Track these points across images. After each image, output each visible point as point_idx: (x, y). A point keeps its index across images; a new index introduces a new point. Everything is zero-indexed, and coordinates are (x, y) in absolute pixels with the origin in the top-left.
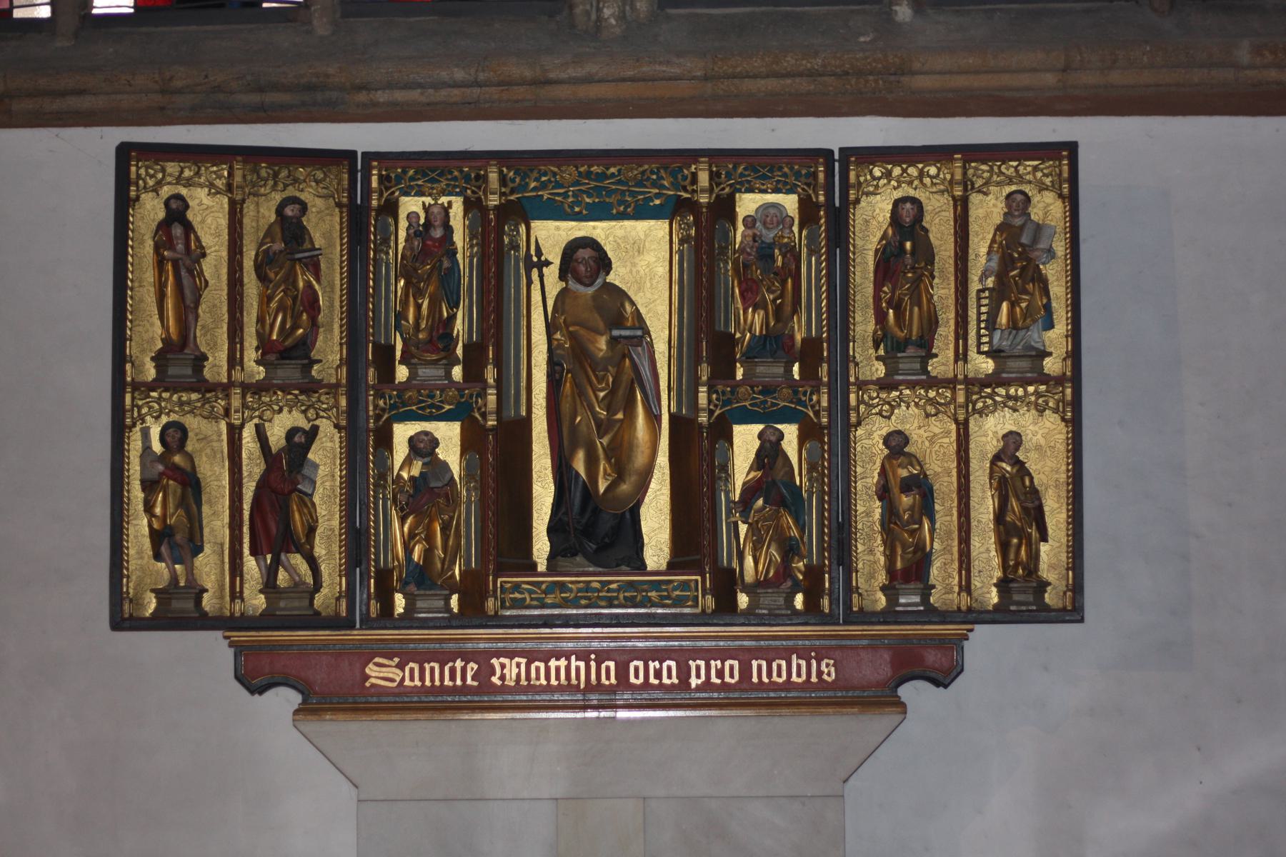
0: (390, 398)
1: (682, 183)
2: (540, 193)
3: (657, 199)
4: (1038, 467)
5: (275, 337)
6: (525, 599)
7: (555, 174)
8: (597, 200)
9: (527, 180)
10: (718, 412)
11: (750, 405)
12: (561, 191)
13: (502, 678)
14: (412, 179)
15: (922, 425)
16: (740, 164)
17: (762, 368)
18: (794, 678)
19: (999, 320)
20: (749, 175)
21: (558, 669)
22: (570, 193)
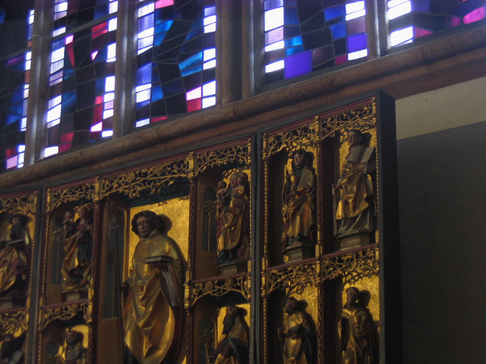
1: (183, 169)
3: (171, 180)
4: (374, 310)
8: (144, 188)
9: (113, 184)
12: (127, 186)
15: (310, 292)
16: (210, 152)
17: (226, 270)
19: (337, 214)
20: (215, 157)
22: (131, 187)
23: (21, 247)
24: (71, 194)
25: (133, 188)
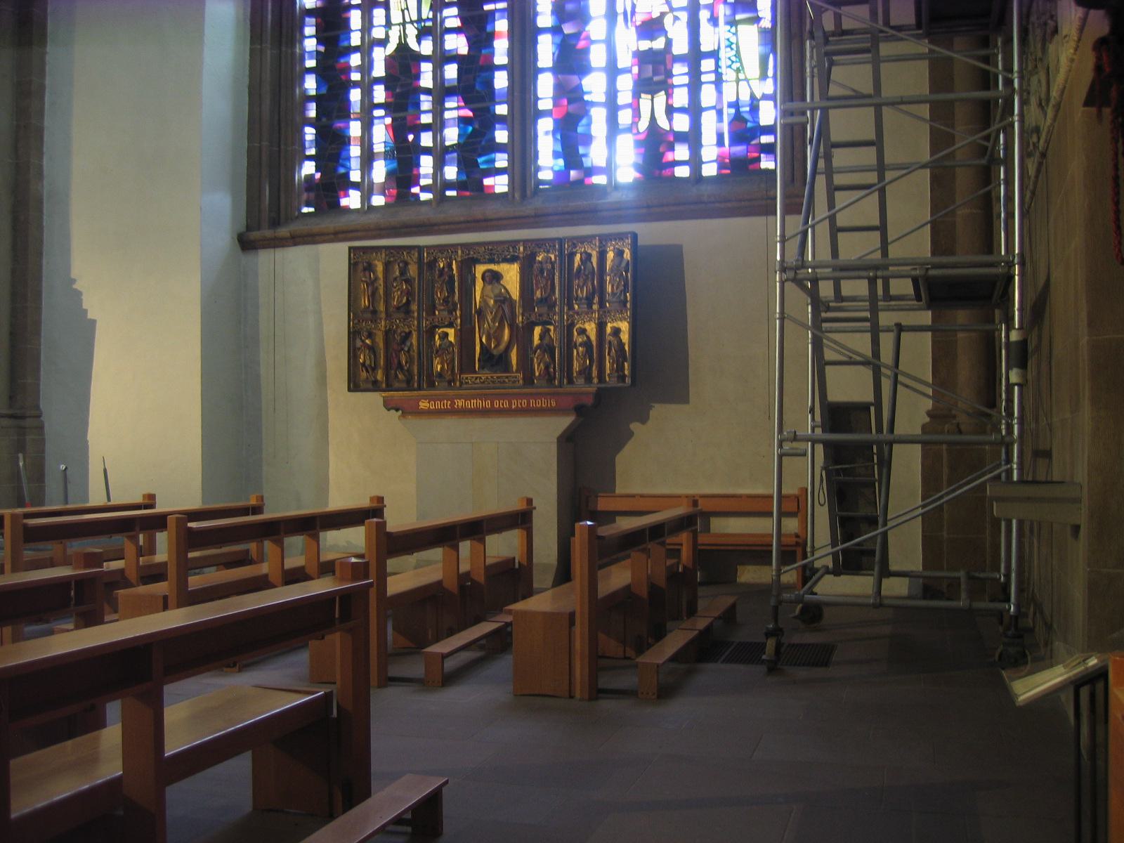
10: (525, 323)
18: (543, 405)
23: (407, 281)
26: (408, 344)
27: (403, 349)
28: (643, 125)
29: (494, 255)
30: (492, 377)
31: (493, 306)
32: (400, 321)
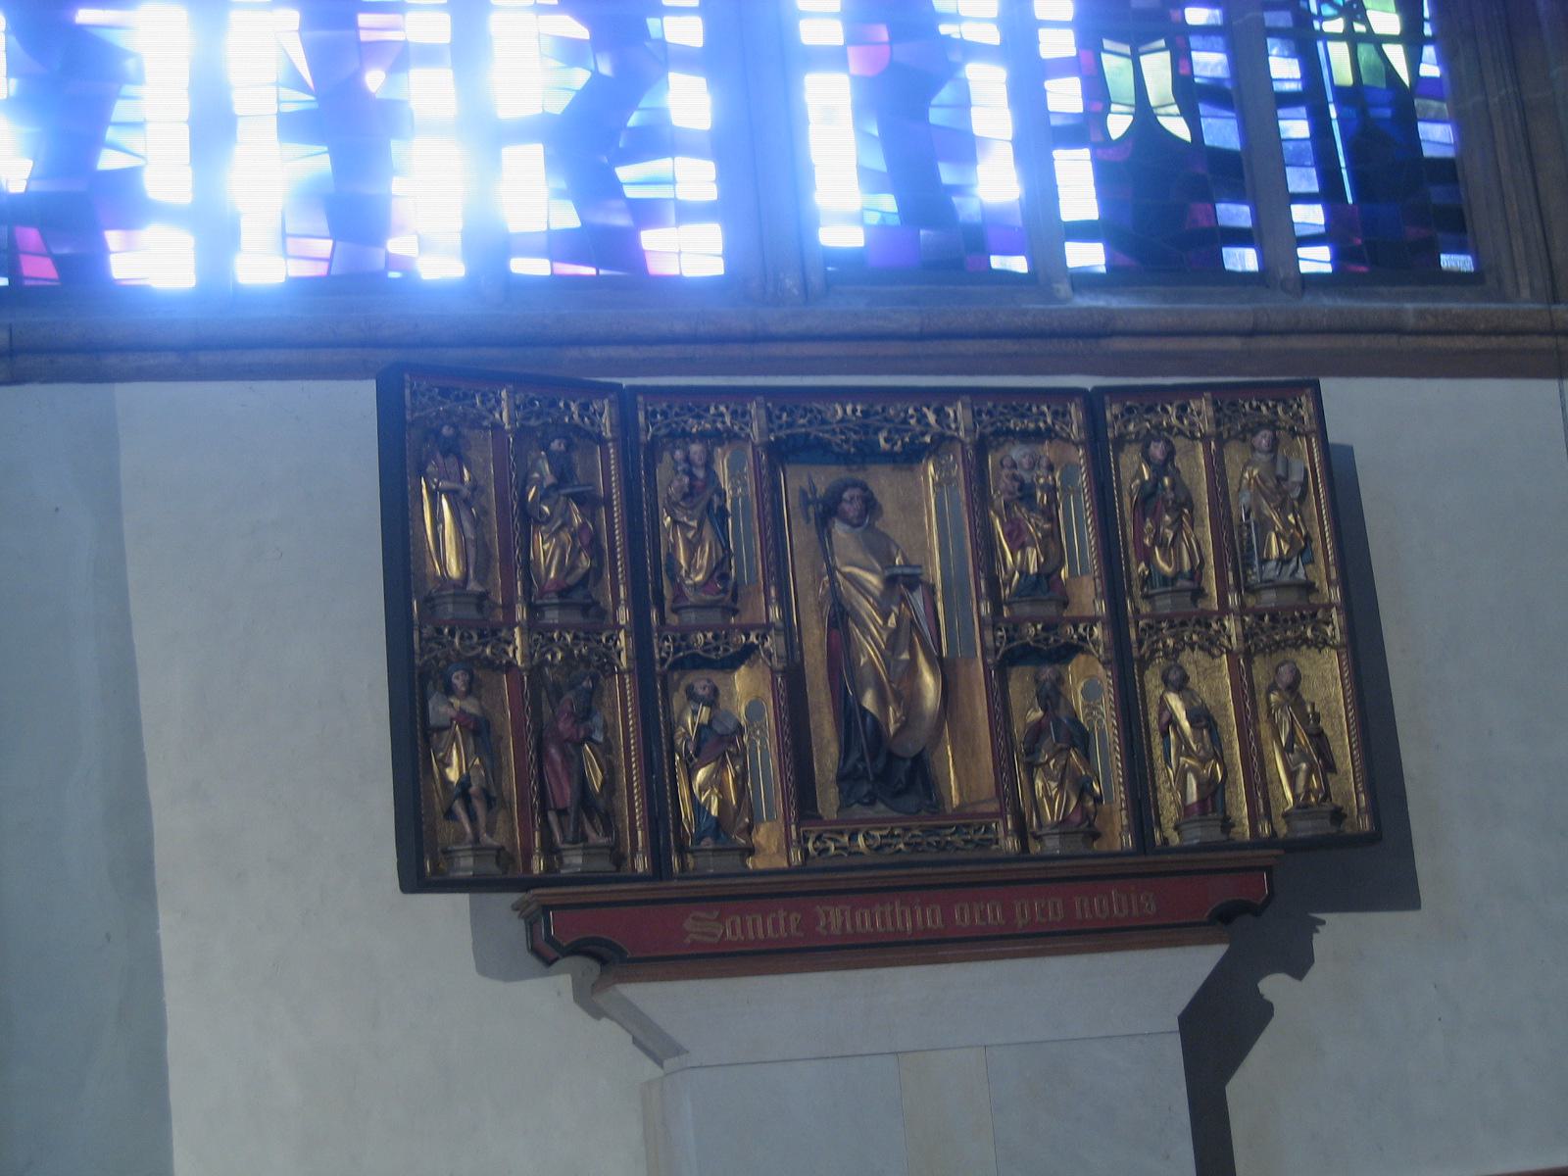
0: (674, 640)
2: (809, 430)
5: (552, 575)
6: (827, 849)
7: (820, 412)
11: (1035, 641)
13: (827, 926)
14: (677, 415)
21: (883, 913)
22: (838, 430)
23: (588, 501)
24: (693, 417)
25: (842, 433)
26: (597, 720)
27: (589, 739)
28: (1118, 124)
29: (878, 430)
30: (906, 829)
31: (883, 594)
32: (575, 637)
